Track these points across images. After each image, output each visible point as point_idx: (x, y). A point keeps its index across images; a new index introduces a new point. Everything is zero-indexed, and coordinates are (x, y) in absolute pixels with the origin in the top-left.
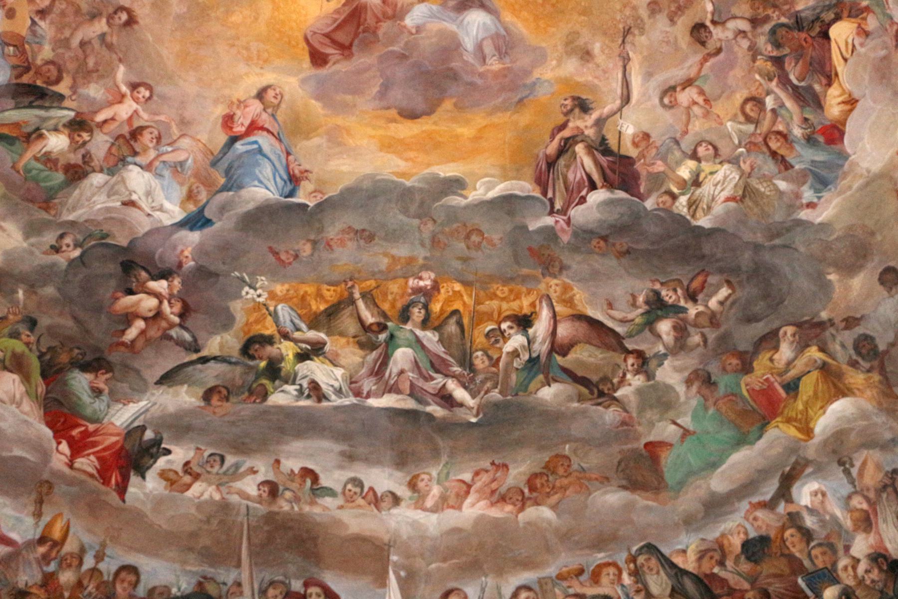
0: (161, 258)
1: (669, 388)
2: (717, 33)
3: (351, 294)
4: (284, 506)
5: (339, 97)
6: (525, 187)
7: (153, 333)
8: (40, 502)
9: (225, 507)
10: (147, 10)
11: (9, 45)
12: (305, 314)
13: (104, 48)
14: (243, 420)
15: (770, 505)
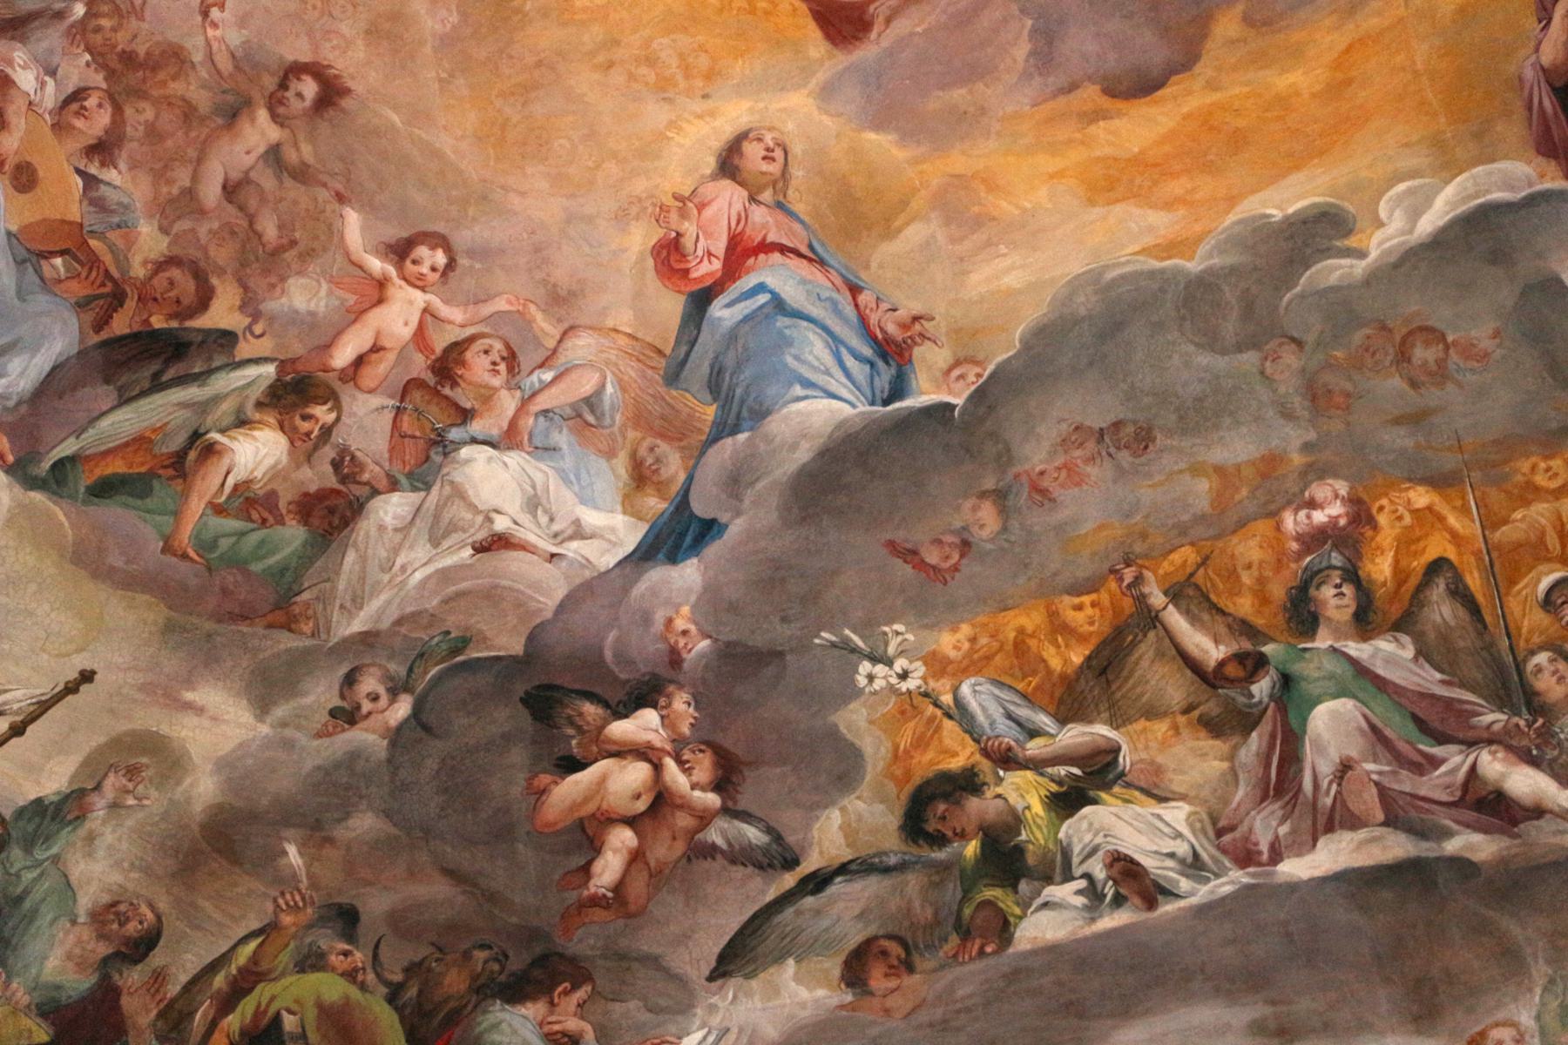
0: (618, 655)
3: (1141, 600)
5: (936, 101)
7: (664, 850)
10: (359, 52)
11: (53, 254)
12: (1036, 689)
13: (289, 182)
14: (968, 1010)
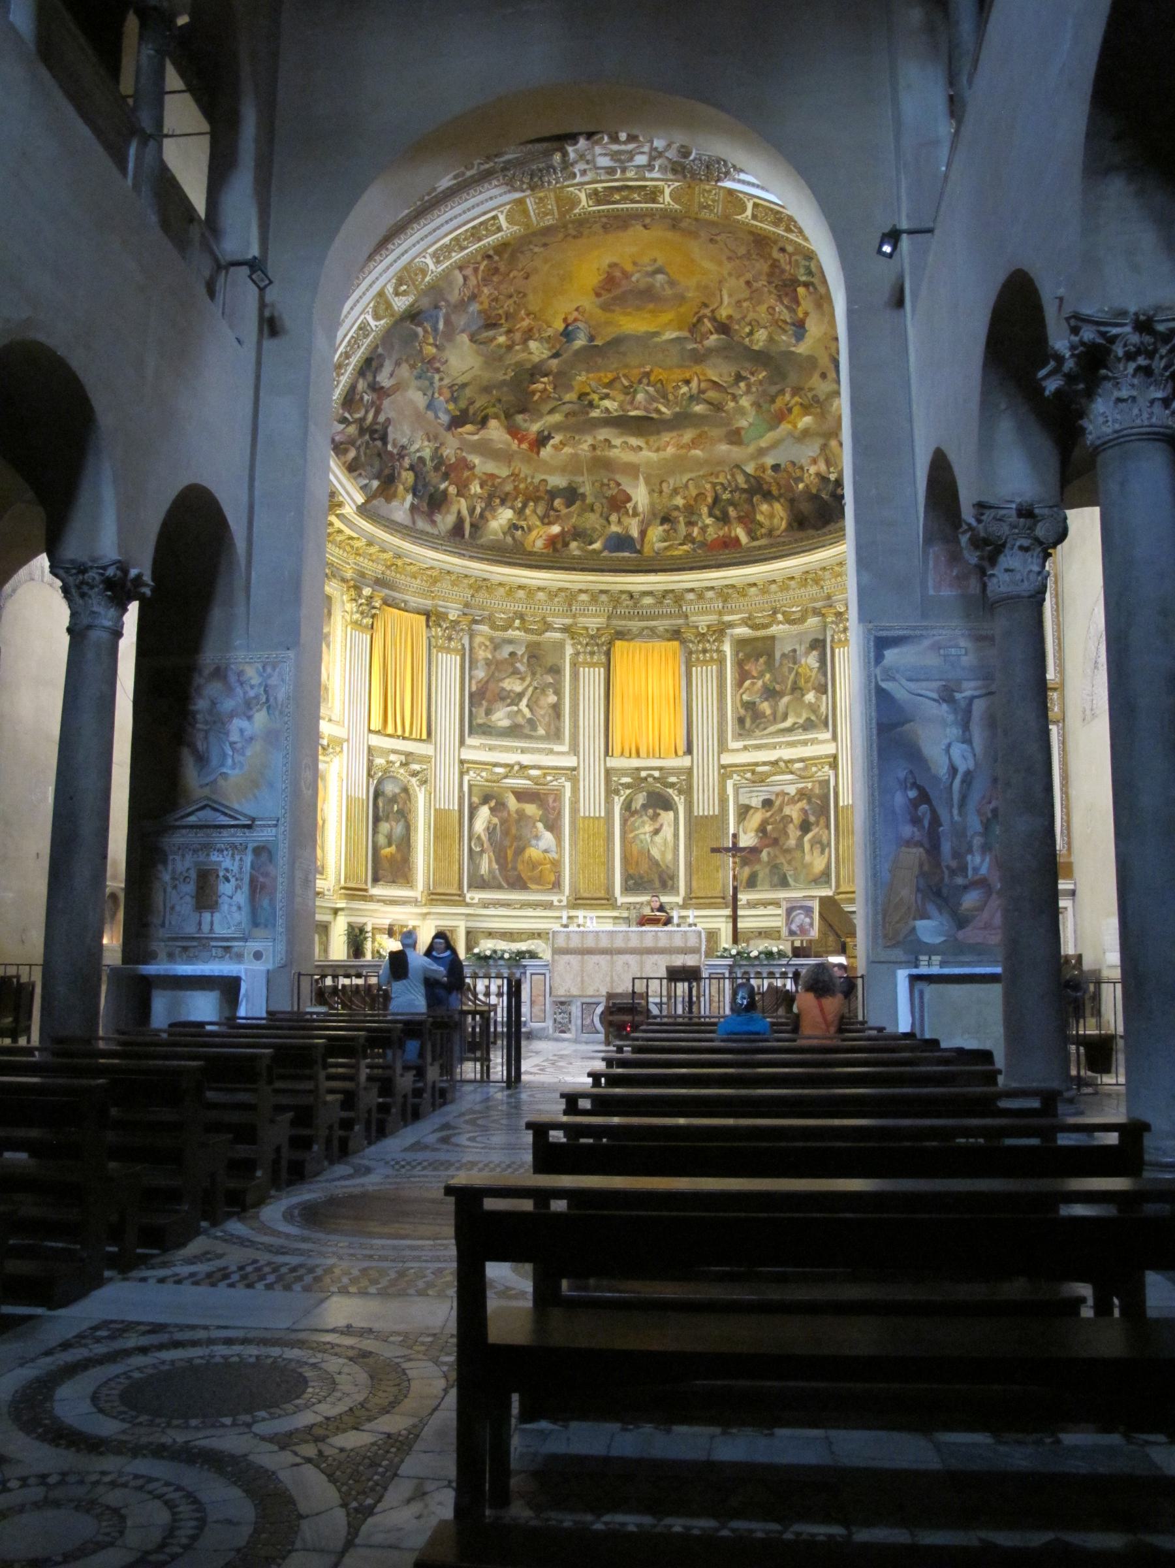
1: (743, 407)
2: (755, 284)
4: (598, 452)
6: (686, 334)
7: (544, 396)
9: (576, 455)
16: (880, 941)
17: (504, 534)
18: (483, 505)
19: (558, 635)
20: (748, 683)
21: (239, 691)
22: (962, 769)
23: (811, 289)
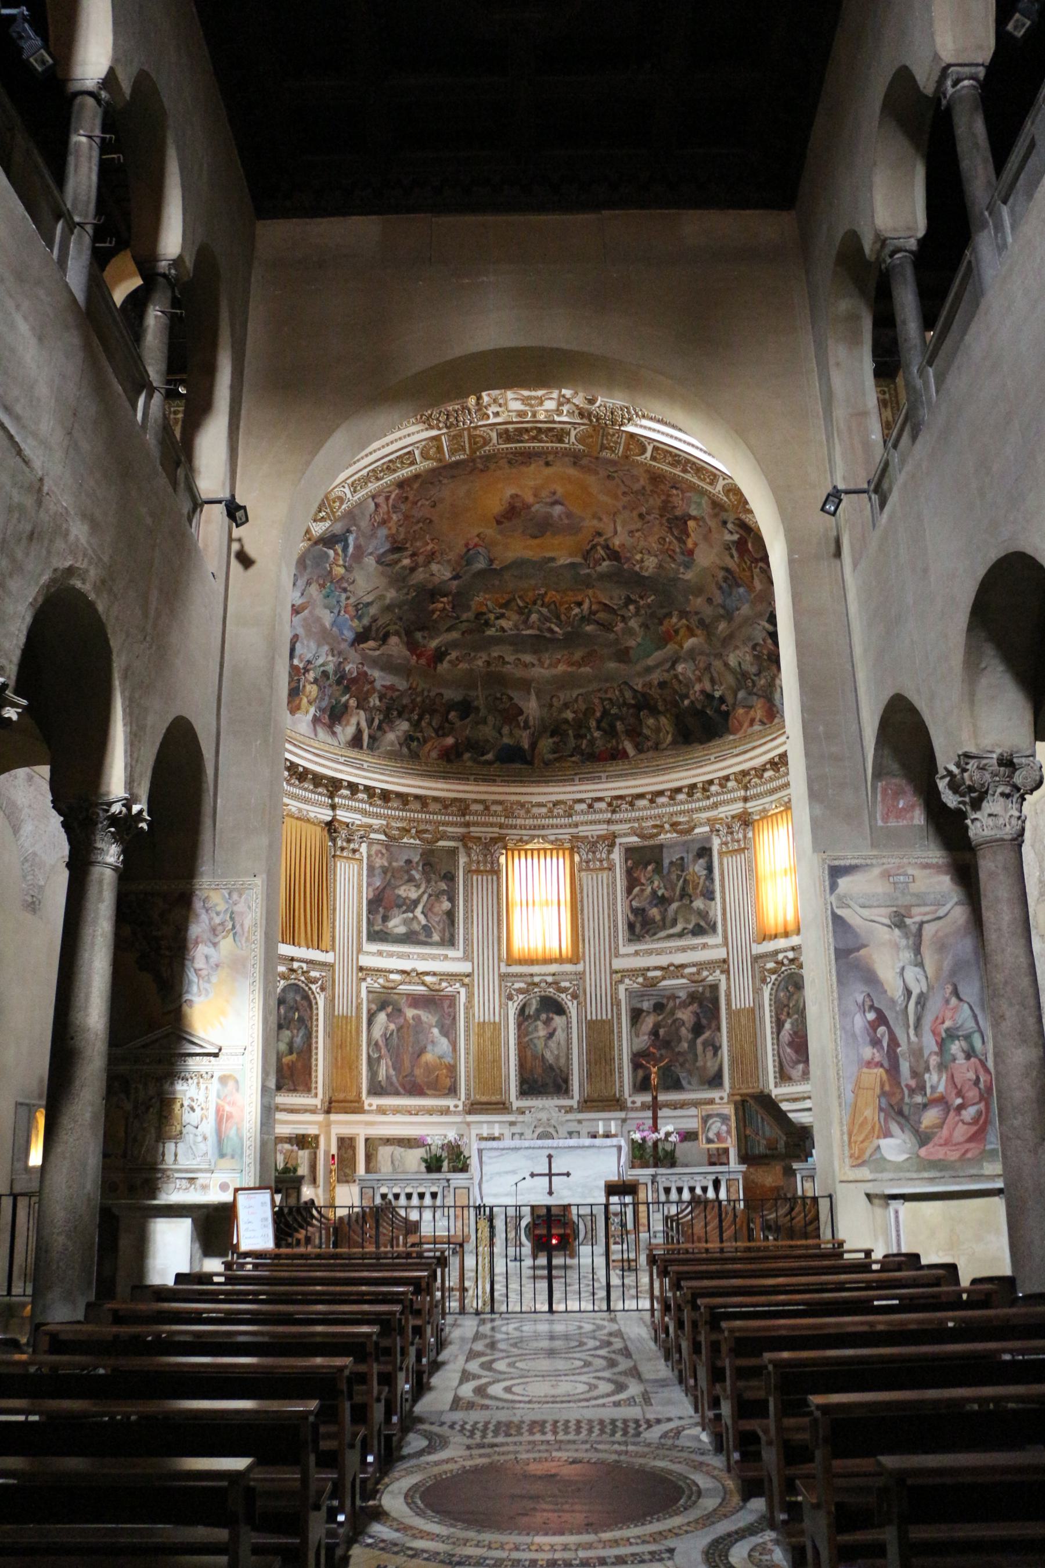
2: (648, 517)
4: (492, 668)
6: (578, 560)
8: (408, 676)
9: (472, 670)
15: (668, 671)
16: (847, 1160)
17: (401, 745)
18: (381, 717)
19: (452, 844)
20: (637, 890)
21: (204, 917)
22: (915, 992)
23: (701, 523)
